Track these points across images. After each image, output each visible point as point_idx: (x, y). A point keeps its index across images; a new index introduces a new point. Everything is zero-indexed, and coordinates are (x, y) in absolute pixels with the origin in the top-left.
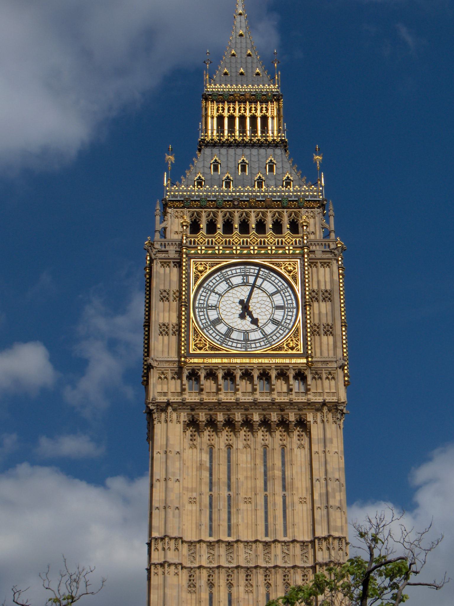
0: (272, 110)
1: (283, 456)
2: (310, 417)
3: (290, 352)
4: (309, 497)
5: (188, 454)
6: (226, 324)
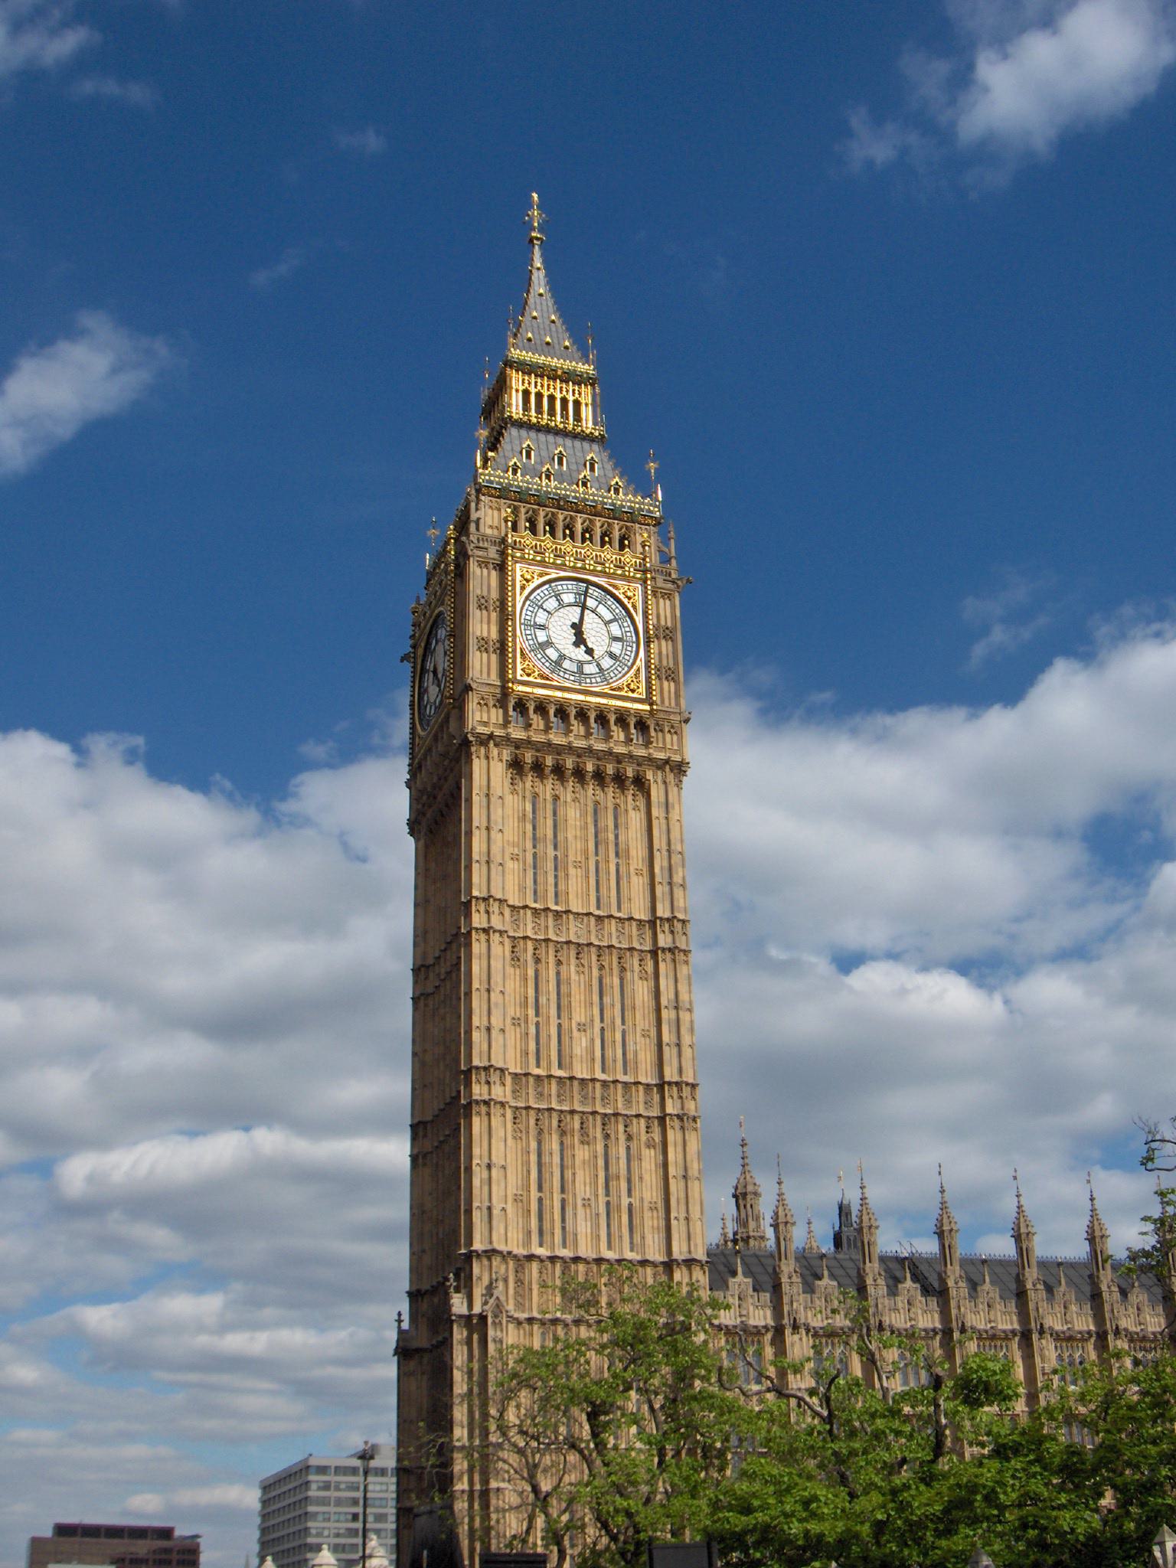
0: (586, 395)
1: (616, 818)
2: (650, 775)
3: (630, 694)
4: (645, 871)
5: (509, 798)
6: (557, 650)
